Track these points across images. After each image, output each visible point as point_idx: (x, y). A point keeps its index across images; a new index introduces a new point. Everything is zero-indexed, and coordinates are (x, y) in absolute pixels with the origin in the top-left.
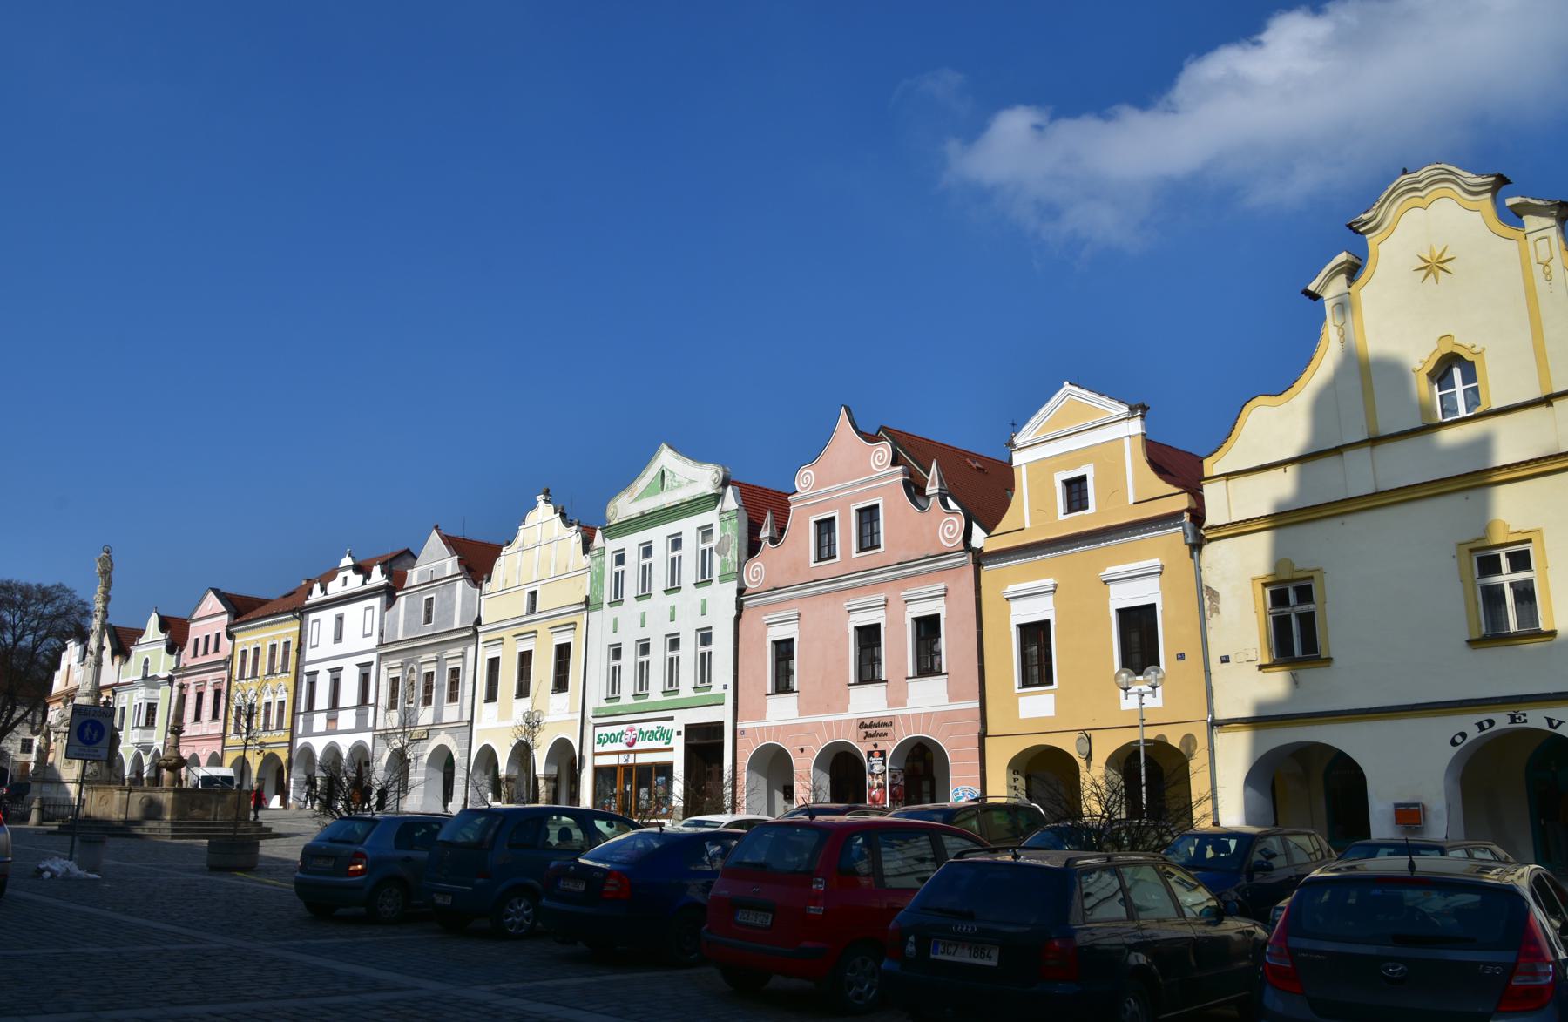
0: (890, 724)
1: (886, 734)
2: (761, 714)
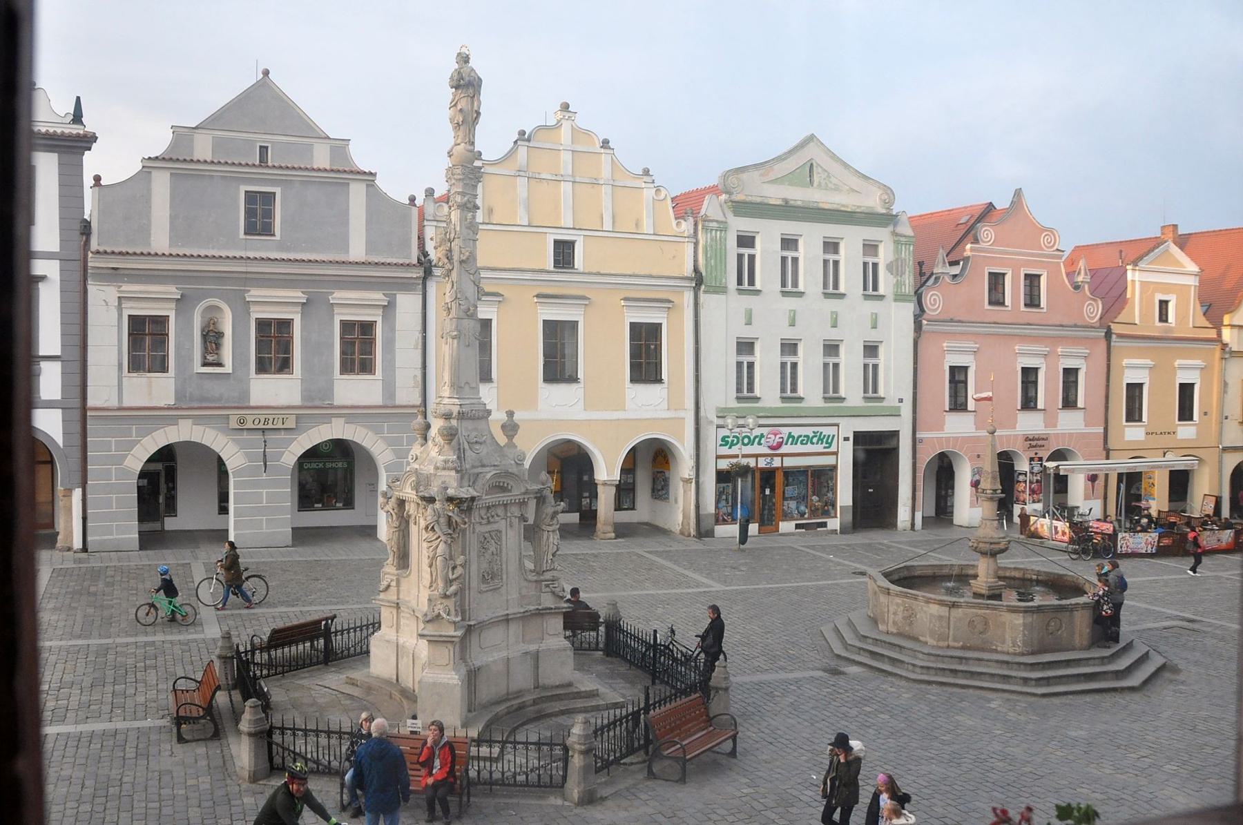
0: (1047, 439)
2: (940, 427)
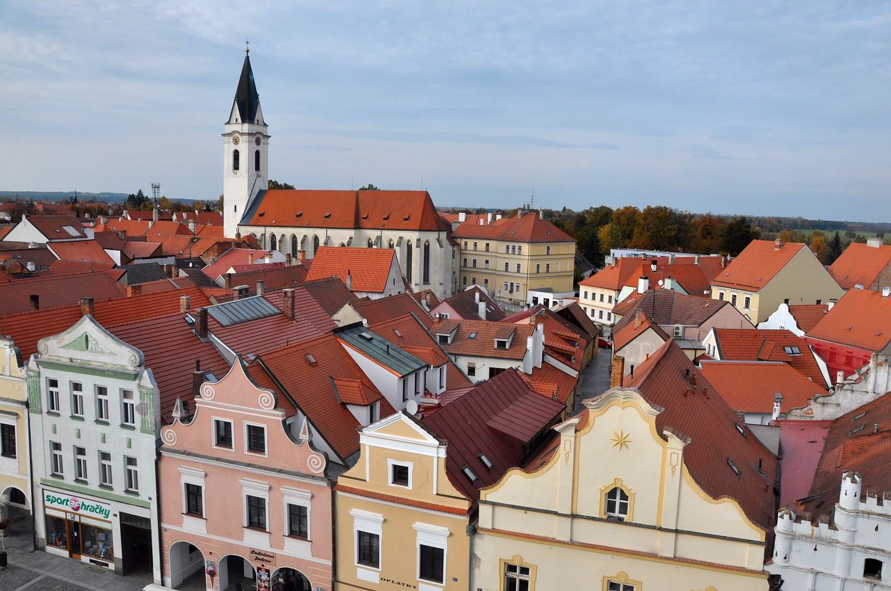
1: (270, 562)
2: (180, 524)
